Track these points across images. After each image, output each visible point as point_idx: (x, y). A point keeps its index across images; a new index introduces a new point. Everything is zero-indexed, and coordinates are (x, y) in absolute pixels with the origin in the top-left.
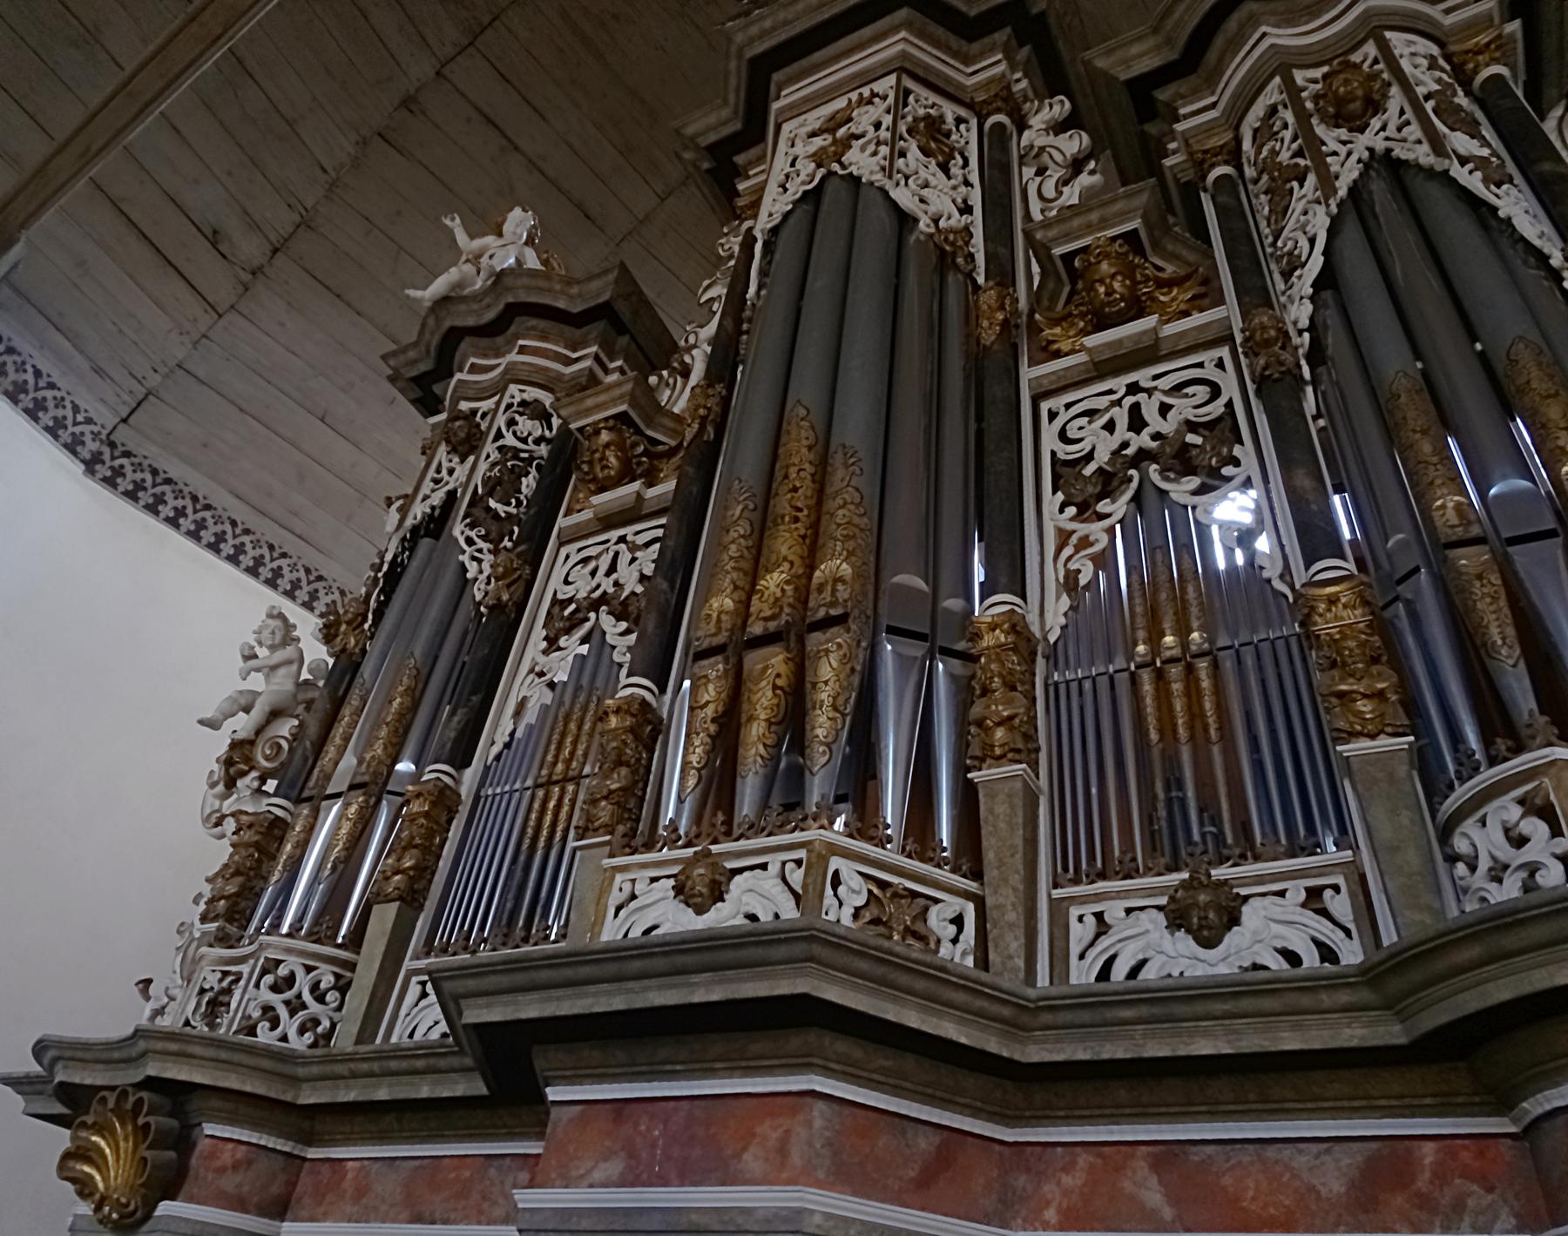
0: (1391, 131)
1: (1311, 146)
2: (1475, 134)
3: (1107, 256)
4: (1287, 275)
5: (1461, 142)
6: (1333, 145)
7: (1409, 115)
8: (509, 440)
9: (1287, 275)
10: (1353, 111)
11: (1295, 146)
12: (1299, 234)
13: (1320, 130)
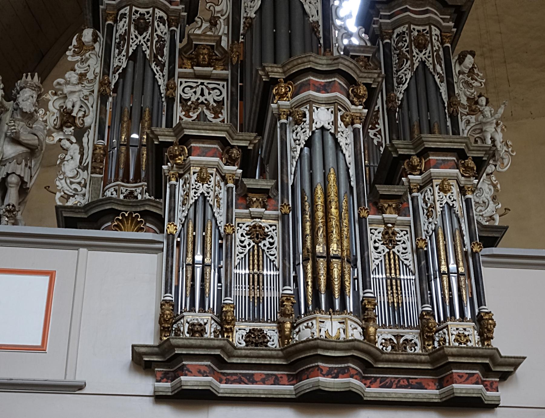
0: (426, 56)
1: (410, 52)
2: (442, 70)
3: (362, 61)
4: (399, 84)
5: (438, 68)
6: (415, 54)
7: (431, 55)
9: (399, 84)
10: (421, 47)
11: (407, 49)
12: (403, 75)
13: (413, 47)
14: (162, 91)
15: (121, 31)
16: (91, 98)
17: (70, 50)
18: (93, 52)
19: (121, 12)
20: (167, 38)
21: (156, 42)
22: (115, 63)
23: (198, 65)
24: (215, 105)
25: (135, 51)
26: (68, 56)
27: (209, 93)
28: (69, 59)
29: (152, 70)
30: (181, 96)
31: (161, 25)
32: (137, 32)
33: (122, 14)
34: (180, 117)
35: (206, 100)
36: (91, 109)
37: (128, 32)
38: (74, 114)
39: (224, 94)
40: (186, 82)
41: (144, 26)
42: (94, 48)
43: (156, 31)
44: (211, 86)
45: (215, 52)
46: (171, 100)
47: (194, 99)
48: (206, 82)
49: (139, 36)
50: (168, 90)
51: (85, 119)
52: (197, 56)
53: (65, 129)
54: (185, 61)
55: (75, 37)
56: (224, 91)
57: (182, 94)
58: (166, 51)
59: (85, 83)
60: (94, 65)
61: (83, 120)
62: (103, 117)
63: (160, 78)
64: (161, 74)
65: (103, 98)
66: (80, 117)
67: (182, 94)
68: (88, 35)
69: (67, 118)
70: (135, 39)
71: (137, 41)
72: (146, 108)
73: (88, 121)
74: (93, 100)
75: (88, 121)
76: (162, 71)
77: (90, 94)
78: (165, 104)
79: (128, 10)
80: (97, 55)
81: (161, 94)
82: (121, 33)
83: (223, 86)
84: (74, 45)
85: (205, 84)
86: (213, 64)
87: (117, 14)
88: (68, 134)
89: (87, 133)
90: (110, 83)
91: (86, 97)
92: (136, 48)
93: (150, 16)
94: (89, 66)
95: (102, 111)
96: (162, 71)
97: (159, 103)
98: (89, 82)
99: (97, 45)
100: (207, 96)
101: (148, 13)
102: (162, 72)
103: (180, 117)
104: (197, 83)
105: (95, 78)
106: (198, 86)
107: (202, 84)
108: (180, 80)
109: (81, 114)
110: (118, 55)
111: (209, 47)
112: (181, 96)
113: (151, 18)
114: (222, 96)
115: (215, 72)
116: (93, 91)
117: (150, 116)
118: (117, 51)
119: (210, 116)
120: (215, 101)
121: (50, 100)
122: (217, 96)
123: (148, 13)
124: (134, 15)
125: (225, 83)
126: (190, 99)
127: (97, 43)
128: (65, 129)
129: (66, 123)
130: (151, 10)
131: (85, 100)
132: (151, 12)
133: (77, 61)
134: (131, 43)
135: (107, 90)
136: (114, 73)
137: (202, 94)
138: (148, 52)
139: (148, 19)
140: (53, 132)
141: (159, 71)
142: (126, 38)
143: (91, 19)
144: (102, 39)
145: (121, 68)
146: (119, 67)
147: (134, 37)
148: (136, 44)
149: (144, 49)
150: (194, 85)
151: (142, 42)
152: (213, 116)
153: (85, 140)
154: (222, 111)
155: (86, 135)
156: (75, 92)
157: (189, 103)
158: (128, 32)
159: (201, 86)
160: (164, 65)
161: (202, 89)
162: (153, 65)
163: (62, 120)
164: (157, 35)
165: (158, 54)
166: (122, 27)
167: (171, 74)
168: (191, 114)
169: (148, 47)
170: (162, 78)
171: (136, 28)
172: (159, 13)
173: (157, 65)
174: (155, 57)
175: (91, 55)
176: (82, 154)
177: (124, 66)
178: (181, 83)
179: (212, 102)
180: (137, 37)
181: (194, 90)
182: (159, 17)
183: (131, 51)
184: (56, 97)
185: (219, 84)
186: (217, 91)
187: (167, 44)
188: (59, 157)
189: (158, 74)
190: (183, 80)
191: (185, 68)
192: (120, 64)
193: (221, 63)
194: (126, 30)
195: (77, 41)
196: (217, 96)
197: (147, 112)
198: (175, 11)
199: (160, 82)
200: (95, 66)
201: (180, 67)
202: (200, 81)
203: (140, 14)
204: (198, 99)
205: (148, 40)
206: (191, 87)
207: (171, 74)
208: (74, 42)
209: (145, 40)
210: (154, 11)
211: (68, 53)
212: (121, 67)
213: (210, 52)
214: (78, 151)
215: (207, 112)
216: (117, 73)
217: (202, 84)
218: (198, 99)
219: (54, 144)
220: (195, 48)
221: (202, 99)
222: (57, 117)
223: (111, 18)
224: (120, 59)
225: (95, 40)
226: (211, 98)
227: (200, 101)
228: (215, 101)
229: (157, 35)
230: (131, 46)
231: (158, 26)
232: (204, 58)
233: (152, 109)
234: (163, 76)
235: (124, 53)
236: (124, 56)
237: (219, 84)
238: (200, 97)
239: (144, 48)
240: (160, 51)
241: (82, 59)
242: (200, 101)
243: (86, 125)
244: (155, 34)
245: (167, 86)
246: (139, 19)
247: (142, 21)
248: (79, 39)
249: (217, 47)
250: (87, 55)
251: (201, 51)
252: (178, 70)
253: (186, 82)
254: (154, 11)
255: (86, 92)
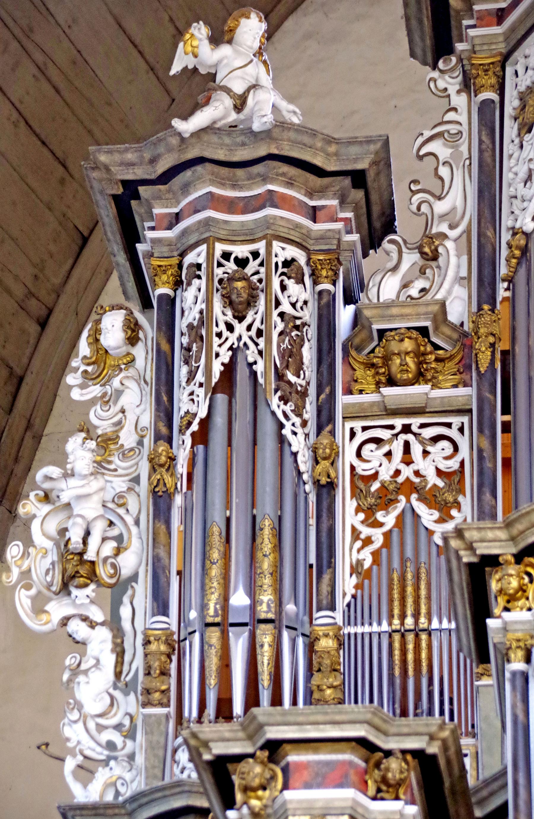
8: (286, 307)
14: (303, 468)
15: (192, 316)
16: (132, 502)
17: (76, 369)
18: (131, 372)
19: (190, 258)
20: (309, 315)
21: (281, 334)
22: (182, 404)
23: (392, 382)
24: (440, 483)
25: (229, 369)
26: (70, 387)
27: (426, 453)
28: (76, 395)
29: (273, 413)
30: (353, 468)
31: (290, 283)
32: (229, 313)
33: (191, 265)
34: (354, 529)
35: (417, 473)
36: (134, 530)
37: (206, 317)
38: (90, 555)
39: (464, 452)
40: (364, 429)
41: (245, 296)
42: (133, 360)
43: (278, 303)
44: (429, 433)
45: (434, 339)
46: (326, 489)
47: (385, 475)
48: (415, 422)
49: (235, 323)
50: (317, 462)
51: (120, 558)
52: (387, 359)
53: (75, 592)
54: (359, 373)
55: (85, 334)
56: (463, 443)
57: (356, 463)
58: (308, 353)
59: (117, 461)
60: (136, 404)
61: (114, 566)
62: (162, 553)
63: (295, 433)
64: (297, 421)
65: (161, 501)
66: (105, 559)
67: (356, 463)
68: (112, 329)
69: (76, 569)
70: (226, 334)
71: (233, 338)
72: (264, 518)
73: (128, 562)
74: (139, 503)
75: (128, 562)
76: (298, 413)
77: (130, 489)
78: (312, 498)
79: (204, 254)
80: (141, 380)
81: (300, 474)
82: (190, 320)
83: (461, 430)
84: (85, 357)
85: (414, 428)
86: (429, 376)
87: (180, 266)
88: (82, 604)
89: (130, 592)
90: (173, 459)
91: (120, 501)
92: (231, 358)
93: (261, 264)
94: (123, 411)
95: (159, 539)
96: (298, 413)
97: (296, 496)
98: (125, 455)
99: (138, 351)
100: (419, 463)
101: (255, 255)
102: (299, 415)
103: (354, 529)
104: (392, 427)
105: (140, 443)
106: (396, 435)
107: (407, 429)
108: (349, 425)
109: (109, 548)
110: (188, 382)
111: (415, 334)
112: (353, 468)
113: (262, 270)
114: (458, 458)
115: (436, 393)
116: (136, 480)
117: (275, 541)
118: (185, 369)
119: (428, 516)
120: (439, 473)
121: (34, 516)
122: (447, 458)
123: (255, 255)
124: (220, 265)
125: (465, 419)
126: (375, 476)
127: (140, 346)
128: (75, 592)
129: (73, 577)
130: (261, 246)
131: (120, 506)
132: (262, 252)
133: (93, 402)
134: (215, 348)
135: (169, 480)
136: (182, 432)
137: (408, 461)
138: (259, 368)
139: (257, 273)
140: (49, 600)
141: (291, 415)
142: (204, 333)
143: (128, 264)
144: (149, 329)
145: (197, 421)
146: (190, 416)
147: (222, 327)
148: (231, 348)
149: (251, 360)
150: (385, 434)
151: (245, 339)
152: (436, 515)
153: (125, 612)
154: (460, 498)
155: (126, 599)
156: (88, 496)
157: (375, 486)
158: (206, 317)
159: (403, 437)
160: (304, 394)
161: (407, 445)
162: (275, 401)
163: (64, 571)
164: (282, 315)
165: (287, 367)
166: (191, 301)
167: (325, 418)
168: (380, 516)
169: (260, 353)
170: (299, 430)
171: (229, 301)
172: (283, 252)
173: (284, 399)
174: (280, 377)
175: (125, 382)
176: (120, 652)
177: (203, 413)
178: (353, 434)
179: (433, 479)
180: (230, 328)
181: (385, 449)
182: (287, 263)
183: (217, 368)
184: (47, 508)
185: (449, 425)
186: (445, 444)
187: (312, 332)
188: (67, 662)
189: (288, 425)
190: (358, 425)
191: (361, 392)
192: (193, 409)
193: (451, 366)
194: (201, 312)
195: (89, 344)
196: (447, 458)
197: (267, 531)
198: (323, 237)
199: (297, 443)
200: (138, 411)
201: (348, 391)
202: (399, 422)
203: (236, 260)
204: (398, 472)
205: (259, 333)
206: (378, 441)
207: (325, 418)
208: (84, 348)
209: (253, 333)
210: (269, 246)
211: (71, 379)
212: (195, 415)
213: (418, 345)
214: (109, 645)
215: (421, 509)
216: (189, 432)
217: (407, 429)
218: (398, 472)
219: (53, 631)
220: (380, 340)
221: (407, 472)
222: (53, 564)
223: (164, 277)
224: (192, 394)
225: (132, 340)
226: (429, 466)
227: (401, 479)
228: (439, 473)
229: (282, 315)
230: (217, 355)
231: (283, 288)
232: (403, 364)
233: (280, 518)
234: (304, 424)
235: (200, 377)
236: (201, 385)
237: (449, 425)
238: (402, 467)
239: (252, 355)
240: (292, 357)
241: (105, 394)
242: (401, 479)
243: (126, 572)
244: (275, 313)
245: (315, 450)
246: (232, 279)
247: (239, 284)
248: (95, 340)
249: (436, 328)
250: (116, 382)
251: (395, 347)
252: (342, 400)
253: (364, 429)
254: (269, 246)
255: (120, 485)
